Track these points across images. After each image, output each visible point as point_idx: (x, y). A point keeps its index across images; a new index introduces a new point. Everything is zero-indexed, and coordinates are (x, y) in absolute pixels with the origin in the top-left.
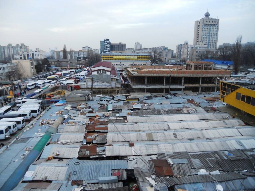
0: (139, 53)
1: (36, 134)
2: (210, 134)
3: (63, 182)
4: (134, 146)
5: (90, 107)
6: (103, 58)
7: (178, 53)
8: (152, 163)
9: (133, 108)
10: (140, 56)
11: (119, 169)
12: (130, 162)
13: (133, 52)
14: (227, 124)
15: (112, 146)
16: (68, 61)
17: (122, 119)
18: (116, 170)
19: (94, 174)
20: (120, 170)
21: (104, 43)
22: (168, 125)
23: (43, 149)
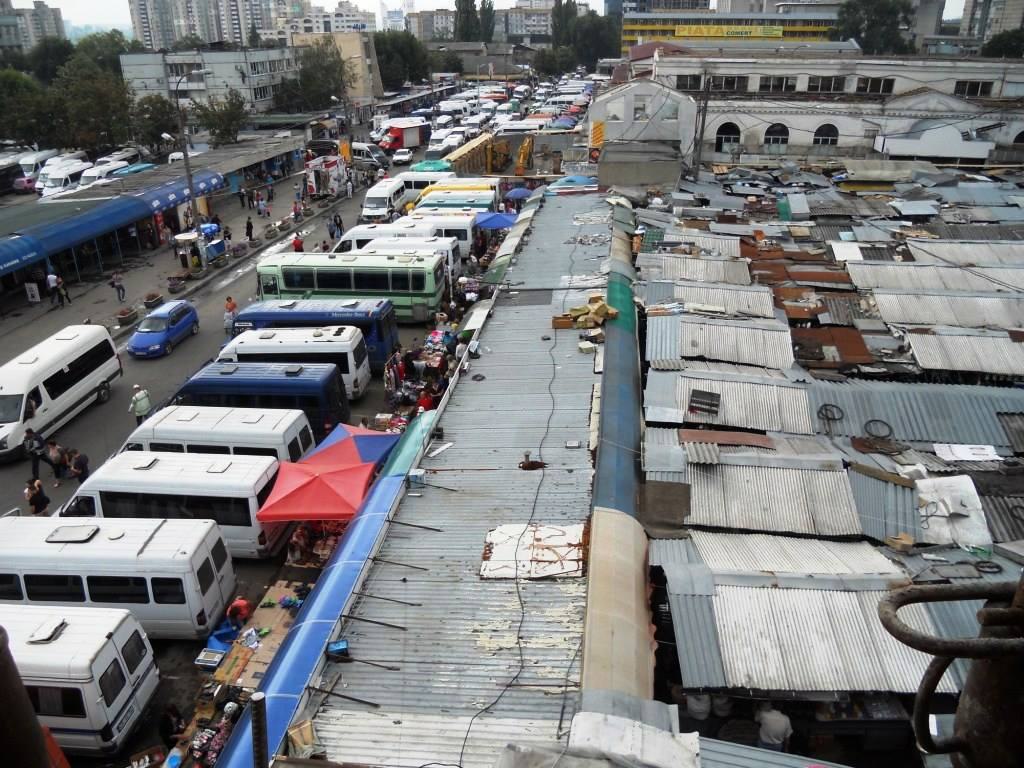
0: (793, 8)
6: (632, 32)
7: (973, 14)
9: (900, 213)
10: (793, 22)
13: (756, 9)
15: (934, 333)
16: (481, 51)
17: (883, 249)
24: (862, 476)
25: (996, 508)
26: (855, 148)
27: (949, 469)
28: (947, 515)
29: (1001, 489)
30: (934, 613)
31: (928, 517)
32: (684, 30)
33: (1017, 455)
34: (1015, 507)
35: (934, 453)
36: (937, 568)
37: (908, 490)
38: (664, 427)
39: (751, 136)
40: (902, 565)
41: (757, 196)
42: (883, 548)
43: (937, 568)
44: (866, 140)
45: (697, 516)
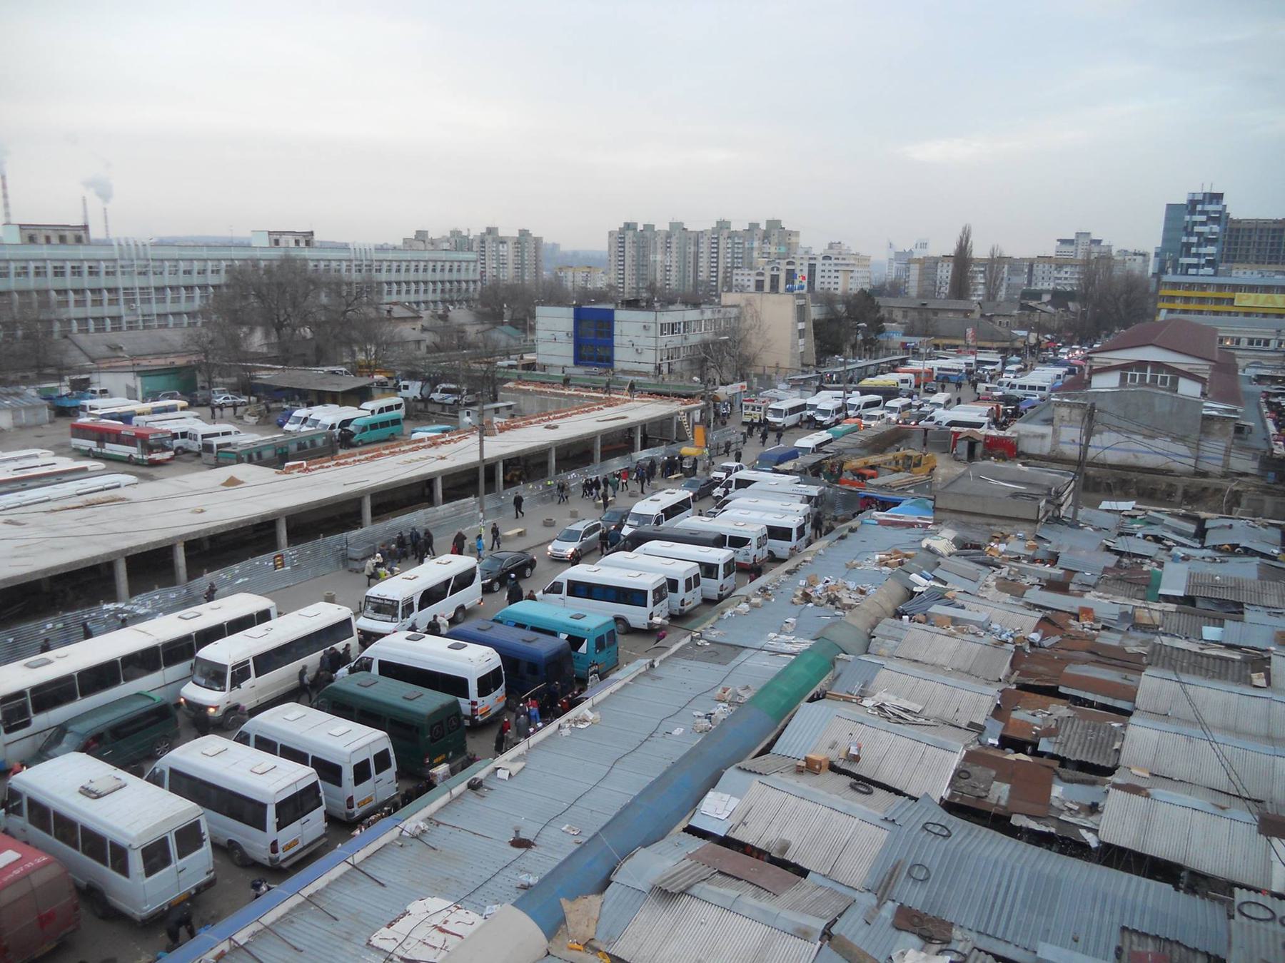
1: (772, 635)
3: (856, 895)
5: (1053, 559)
6: (1172, 299)
11: (1167, 940)
12: (1250, 926)
15: (1148, 796)
16: (972, 311)
17: (1233, 660)
18: (1150, 941)
19: (1015, 913)
20: (1175, 946)
21: (1187, 218)
23: (793, 716)
32: (1249, 298)
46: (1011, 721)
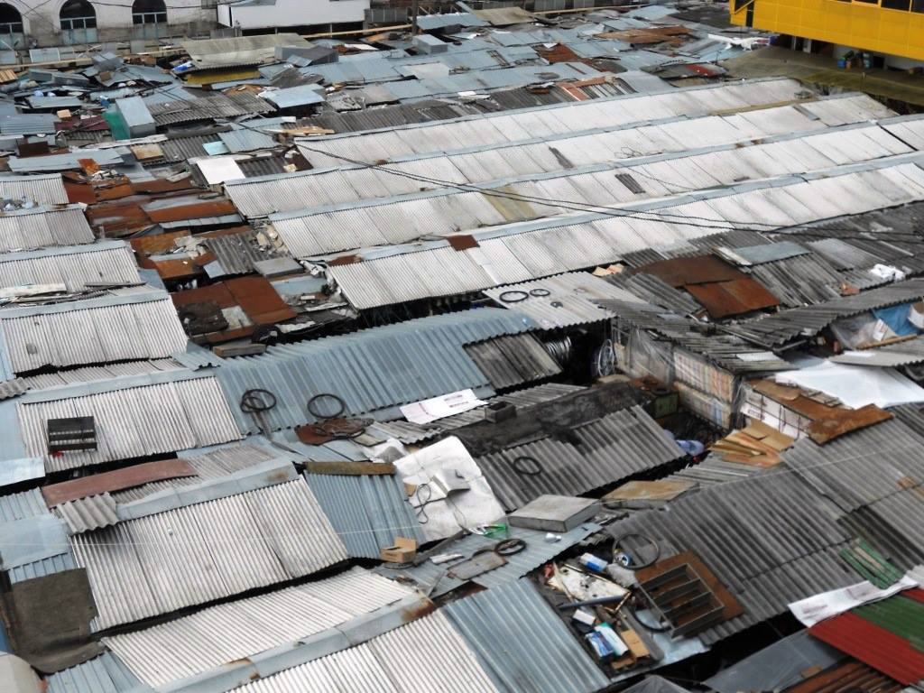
2: (779, 158)
4: (478, 246)
8: (649, 278)
9: (276, 106)
11: (498, 337)
14: (818, 119)
15: (361, 260)
17: (267, 158)
18: (486, 344)
22: (555, 151)
24: (325, 478)
25: (496, 467)
26: (193, 24)
27: (429, 435)
28: (445, 496)
29: (496, 442)
30: (470, 633)
31: (422, 506)
33: (500, 392)
34: (517, 460)
35: (404, 419)
36: (453, 571)
37: (387, 478)
38: (26, 490)
39: (39, 21)
40: (411, 581)
41: (71, 109)
42: (382, 567)
43: (453, 571)
44: (204, 12)
45: (109, 612)
46: (157, 265)
